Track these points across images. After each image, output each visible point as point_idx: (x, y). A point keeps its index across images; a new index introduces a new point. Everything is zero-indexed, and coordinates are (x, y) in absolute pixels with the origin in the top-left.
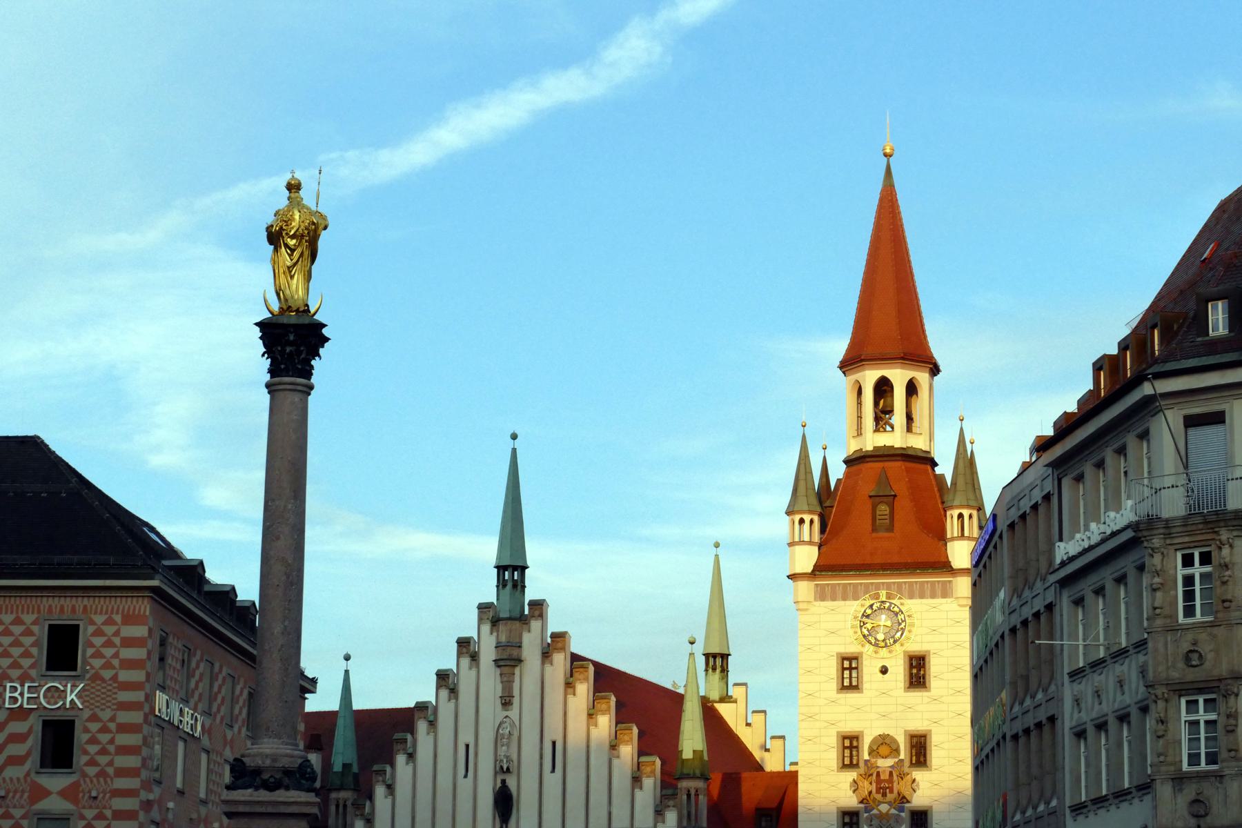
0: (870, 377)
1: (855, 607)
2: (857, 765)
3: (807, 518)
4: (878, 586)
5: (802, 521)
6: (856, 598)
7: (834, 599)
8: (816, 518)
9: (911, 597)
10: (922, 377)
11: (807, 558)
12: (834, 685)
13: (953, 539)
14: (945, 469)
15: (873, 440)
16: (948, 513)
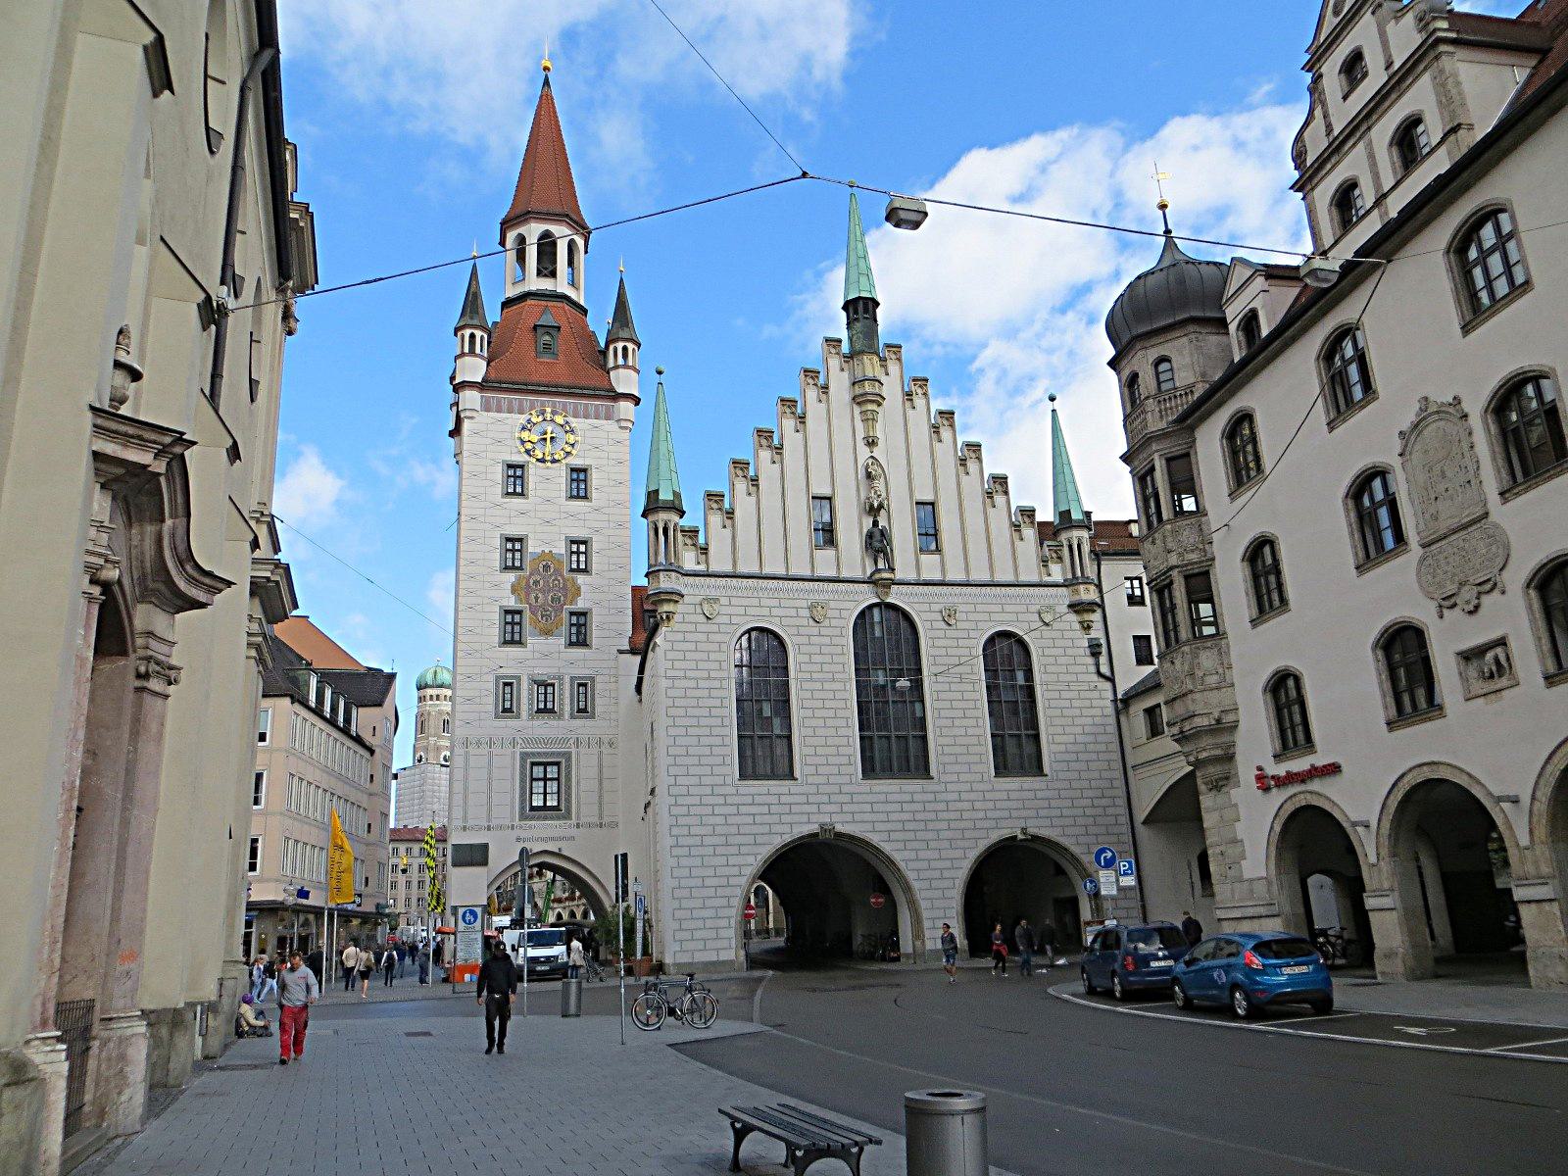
0: (533, 231)
1: (522, 419)
2: (521, 568)
3: (478, 333)
4: (543, 404)
5: (472, 336)
6: (521, 412)
7: (499, 411)
8: (486, 336)
9: (576, 416)
10: (580, 242)
11: (475, 369)
12: (499, 490)
13: (616, 367)
14: (599, 324)
15: (536, 283)
16: (611, 348)
